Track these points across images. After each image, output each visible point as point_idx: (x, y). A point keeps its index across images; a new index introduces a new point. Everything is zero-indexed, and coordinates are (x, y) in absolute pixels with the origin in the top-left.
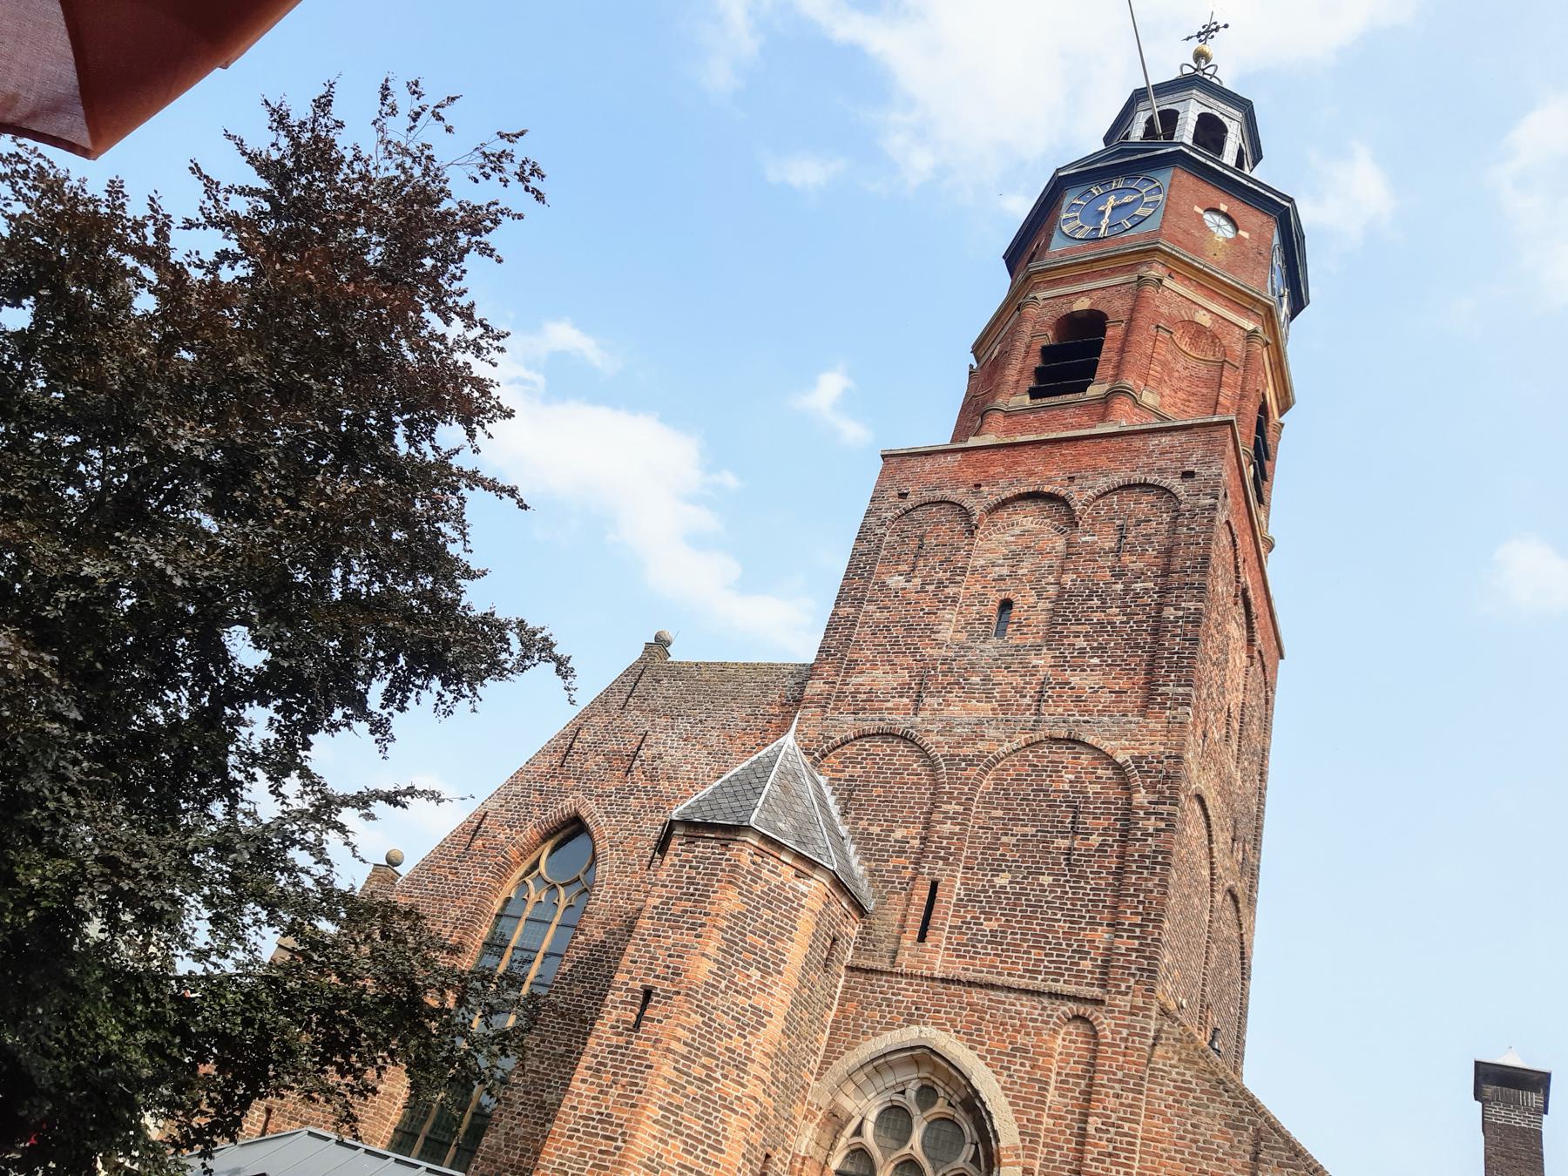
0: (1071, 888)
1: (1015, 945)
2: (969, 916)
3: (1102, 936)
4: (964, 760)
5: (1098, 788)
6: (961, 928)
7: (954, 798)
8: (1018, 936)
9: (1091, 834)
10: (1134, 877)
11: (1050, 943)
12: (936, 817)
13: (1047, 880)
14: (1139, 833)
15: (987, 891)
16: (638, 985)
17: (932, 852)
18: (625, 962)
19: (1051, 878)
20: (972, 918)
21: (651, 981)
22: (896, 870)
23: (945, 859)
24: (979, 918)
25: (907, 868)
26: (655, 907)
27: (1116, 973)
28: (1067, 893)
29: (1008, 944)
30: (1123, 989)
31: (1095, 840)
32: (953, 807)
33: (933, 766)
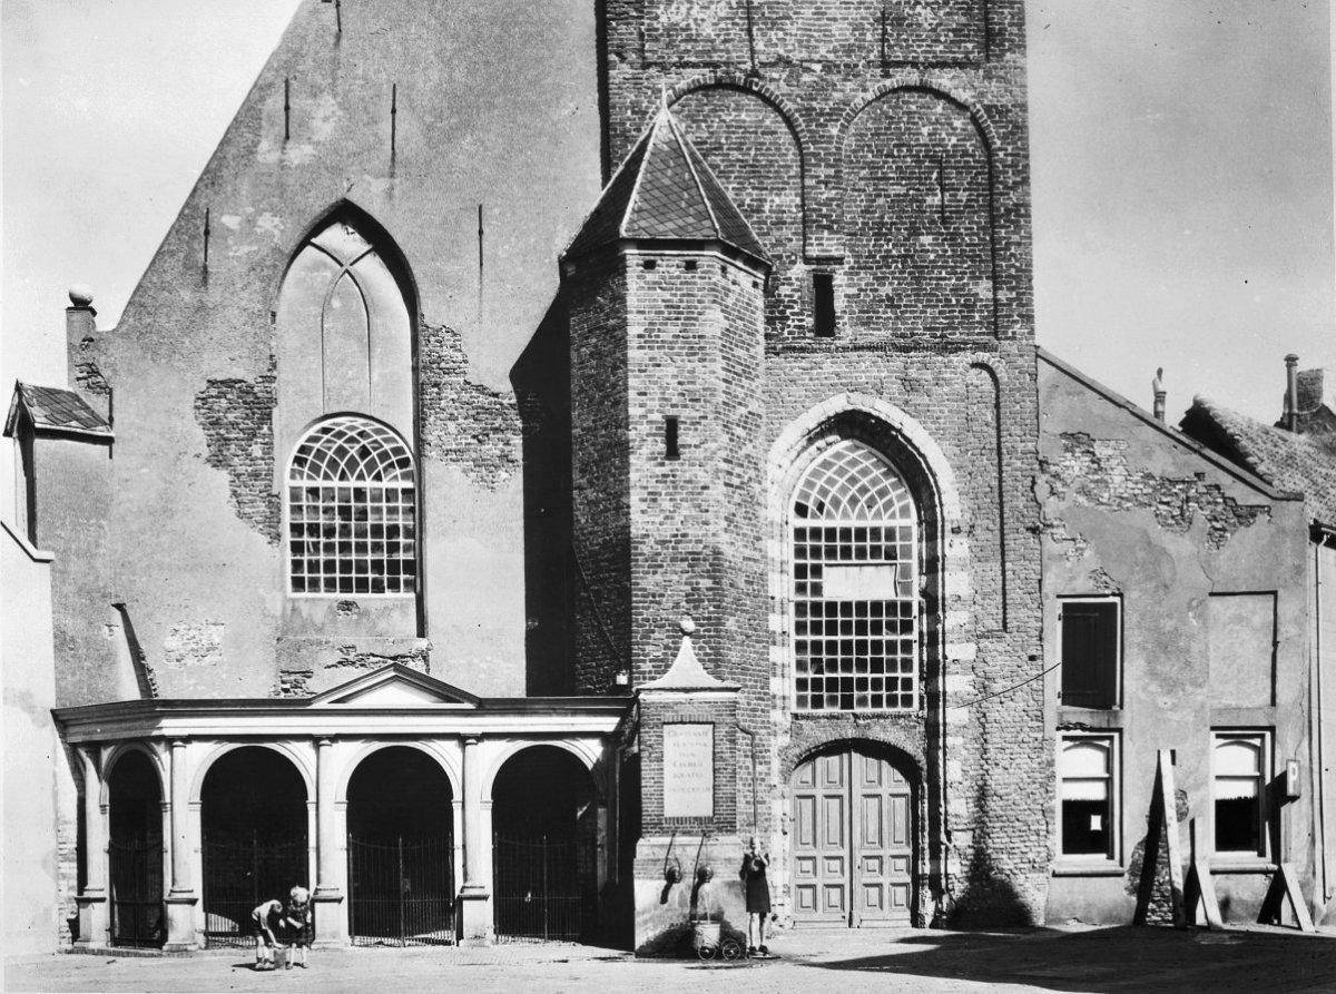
0: (950, 245)
1: (911, 306)
2: (863, 283)
3: (983, 289)
4: (821, 114)
5: (954, 140)
6: (858, 296)
7: (821, 160)
8: (913, 298)
9: (959, 190)
10: (1003, 231)
11: (941, 301)
12: (808, 182)
13: (926, 240)
14: (1001, 187)
15: (875, 256)
16: (657, 417)
17: (815, 221)
18: (632, 394)
19: (930, 237)
20: (866, 285)
21: (672, 412)
22: (779, 243)
23: (829, 228)
24: (873, 284)
25: (791, 240)
26: (640, 336)
27: (1003, 322)
28: (946, 251)
29: (905, 306)
30: (1010, 334)
31: (963, 196)
32: (823, 172)
33: (789, 121)
